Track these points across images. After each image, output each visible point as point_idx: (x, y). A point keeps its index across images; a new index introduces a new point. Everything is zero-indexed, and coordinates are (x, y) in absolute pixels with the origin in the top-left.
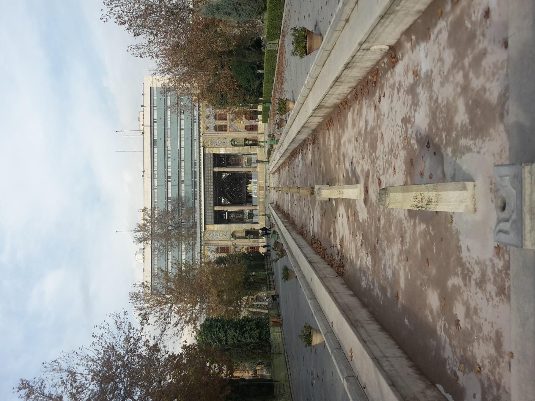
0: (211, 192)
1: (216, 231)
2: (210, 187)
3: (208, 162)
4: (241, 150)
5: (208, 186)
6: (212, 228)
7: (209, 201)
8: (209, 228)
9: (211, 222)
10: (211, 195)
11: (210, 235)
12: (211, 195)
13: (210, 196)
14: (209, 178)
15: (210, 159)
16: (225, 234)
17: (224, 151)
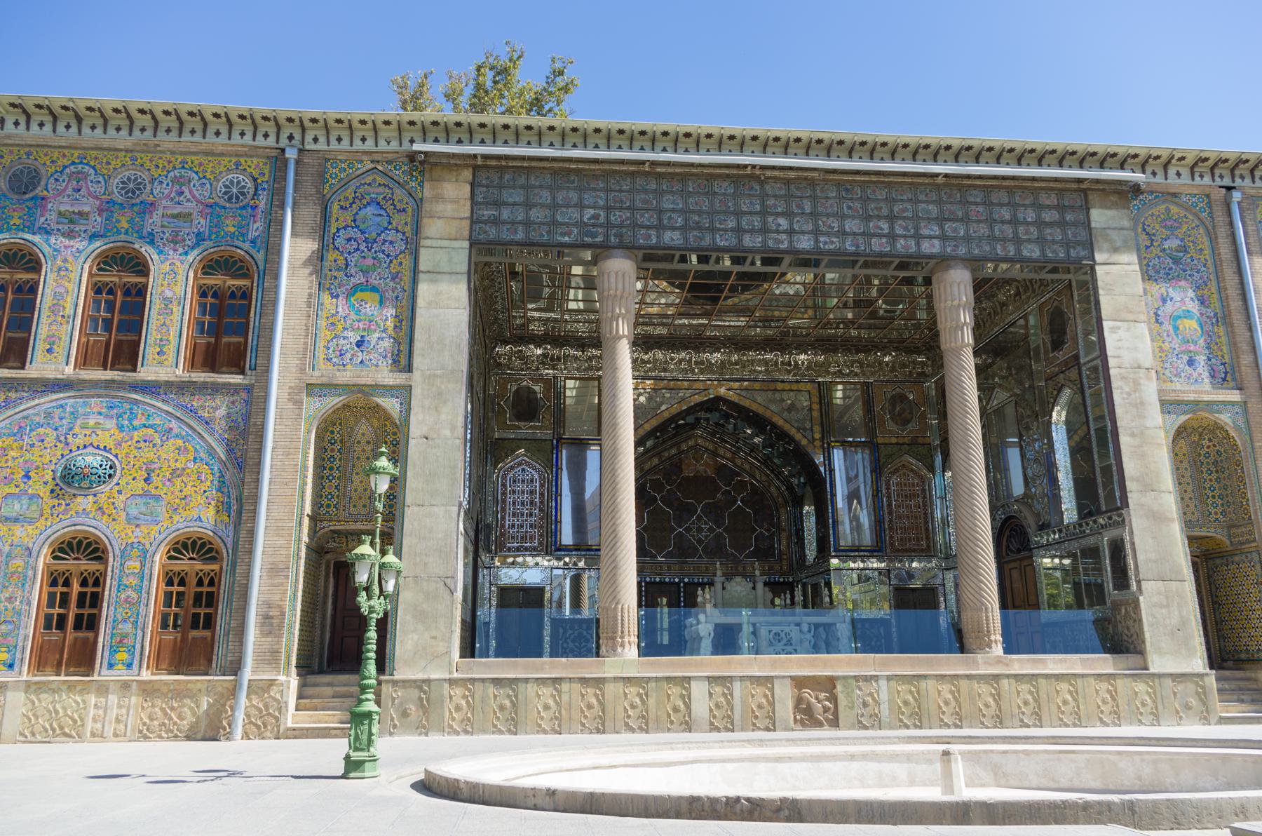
0: (764, 231)
1: (407, 261)
2: (809, 227)
3: (1014, 222)
4: (1148, 499)
5: (814, 215)
6: (432, 228)
7: (685, 212)
8: (439, 198)
9: (495, 221)
10: (738, 230)
11: (370, 210)
12: (738, 230)
13: (731, 224)
14: (885, 226)
15: (1041, 241)
16: (373, 338)
17: (1127, 358)
